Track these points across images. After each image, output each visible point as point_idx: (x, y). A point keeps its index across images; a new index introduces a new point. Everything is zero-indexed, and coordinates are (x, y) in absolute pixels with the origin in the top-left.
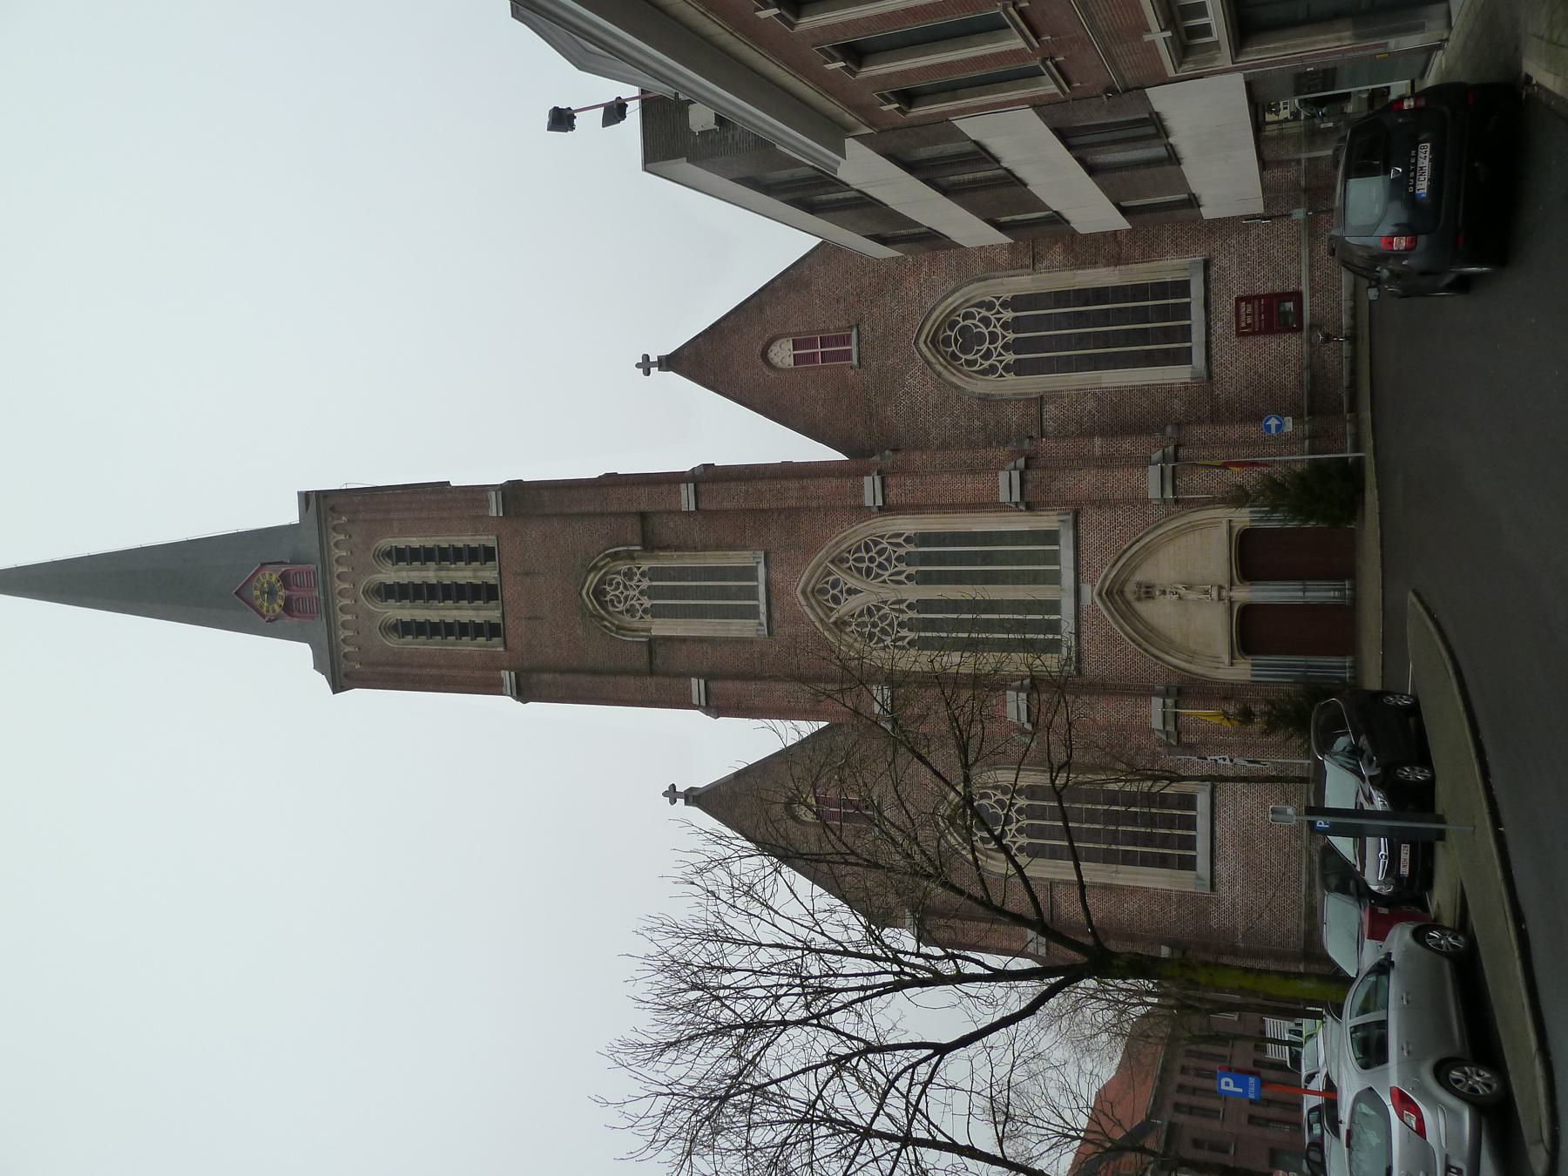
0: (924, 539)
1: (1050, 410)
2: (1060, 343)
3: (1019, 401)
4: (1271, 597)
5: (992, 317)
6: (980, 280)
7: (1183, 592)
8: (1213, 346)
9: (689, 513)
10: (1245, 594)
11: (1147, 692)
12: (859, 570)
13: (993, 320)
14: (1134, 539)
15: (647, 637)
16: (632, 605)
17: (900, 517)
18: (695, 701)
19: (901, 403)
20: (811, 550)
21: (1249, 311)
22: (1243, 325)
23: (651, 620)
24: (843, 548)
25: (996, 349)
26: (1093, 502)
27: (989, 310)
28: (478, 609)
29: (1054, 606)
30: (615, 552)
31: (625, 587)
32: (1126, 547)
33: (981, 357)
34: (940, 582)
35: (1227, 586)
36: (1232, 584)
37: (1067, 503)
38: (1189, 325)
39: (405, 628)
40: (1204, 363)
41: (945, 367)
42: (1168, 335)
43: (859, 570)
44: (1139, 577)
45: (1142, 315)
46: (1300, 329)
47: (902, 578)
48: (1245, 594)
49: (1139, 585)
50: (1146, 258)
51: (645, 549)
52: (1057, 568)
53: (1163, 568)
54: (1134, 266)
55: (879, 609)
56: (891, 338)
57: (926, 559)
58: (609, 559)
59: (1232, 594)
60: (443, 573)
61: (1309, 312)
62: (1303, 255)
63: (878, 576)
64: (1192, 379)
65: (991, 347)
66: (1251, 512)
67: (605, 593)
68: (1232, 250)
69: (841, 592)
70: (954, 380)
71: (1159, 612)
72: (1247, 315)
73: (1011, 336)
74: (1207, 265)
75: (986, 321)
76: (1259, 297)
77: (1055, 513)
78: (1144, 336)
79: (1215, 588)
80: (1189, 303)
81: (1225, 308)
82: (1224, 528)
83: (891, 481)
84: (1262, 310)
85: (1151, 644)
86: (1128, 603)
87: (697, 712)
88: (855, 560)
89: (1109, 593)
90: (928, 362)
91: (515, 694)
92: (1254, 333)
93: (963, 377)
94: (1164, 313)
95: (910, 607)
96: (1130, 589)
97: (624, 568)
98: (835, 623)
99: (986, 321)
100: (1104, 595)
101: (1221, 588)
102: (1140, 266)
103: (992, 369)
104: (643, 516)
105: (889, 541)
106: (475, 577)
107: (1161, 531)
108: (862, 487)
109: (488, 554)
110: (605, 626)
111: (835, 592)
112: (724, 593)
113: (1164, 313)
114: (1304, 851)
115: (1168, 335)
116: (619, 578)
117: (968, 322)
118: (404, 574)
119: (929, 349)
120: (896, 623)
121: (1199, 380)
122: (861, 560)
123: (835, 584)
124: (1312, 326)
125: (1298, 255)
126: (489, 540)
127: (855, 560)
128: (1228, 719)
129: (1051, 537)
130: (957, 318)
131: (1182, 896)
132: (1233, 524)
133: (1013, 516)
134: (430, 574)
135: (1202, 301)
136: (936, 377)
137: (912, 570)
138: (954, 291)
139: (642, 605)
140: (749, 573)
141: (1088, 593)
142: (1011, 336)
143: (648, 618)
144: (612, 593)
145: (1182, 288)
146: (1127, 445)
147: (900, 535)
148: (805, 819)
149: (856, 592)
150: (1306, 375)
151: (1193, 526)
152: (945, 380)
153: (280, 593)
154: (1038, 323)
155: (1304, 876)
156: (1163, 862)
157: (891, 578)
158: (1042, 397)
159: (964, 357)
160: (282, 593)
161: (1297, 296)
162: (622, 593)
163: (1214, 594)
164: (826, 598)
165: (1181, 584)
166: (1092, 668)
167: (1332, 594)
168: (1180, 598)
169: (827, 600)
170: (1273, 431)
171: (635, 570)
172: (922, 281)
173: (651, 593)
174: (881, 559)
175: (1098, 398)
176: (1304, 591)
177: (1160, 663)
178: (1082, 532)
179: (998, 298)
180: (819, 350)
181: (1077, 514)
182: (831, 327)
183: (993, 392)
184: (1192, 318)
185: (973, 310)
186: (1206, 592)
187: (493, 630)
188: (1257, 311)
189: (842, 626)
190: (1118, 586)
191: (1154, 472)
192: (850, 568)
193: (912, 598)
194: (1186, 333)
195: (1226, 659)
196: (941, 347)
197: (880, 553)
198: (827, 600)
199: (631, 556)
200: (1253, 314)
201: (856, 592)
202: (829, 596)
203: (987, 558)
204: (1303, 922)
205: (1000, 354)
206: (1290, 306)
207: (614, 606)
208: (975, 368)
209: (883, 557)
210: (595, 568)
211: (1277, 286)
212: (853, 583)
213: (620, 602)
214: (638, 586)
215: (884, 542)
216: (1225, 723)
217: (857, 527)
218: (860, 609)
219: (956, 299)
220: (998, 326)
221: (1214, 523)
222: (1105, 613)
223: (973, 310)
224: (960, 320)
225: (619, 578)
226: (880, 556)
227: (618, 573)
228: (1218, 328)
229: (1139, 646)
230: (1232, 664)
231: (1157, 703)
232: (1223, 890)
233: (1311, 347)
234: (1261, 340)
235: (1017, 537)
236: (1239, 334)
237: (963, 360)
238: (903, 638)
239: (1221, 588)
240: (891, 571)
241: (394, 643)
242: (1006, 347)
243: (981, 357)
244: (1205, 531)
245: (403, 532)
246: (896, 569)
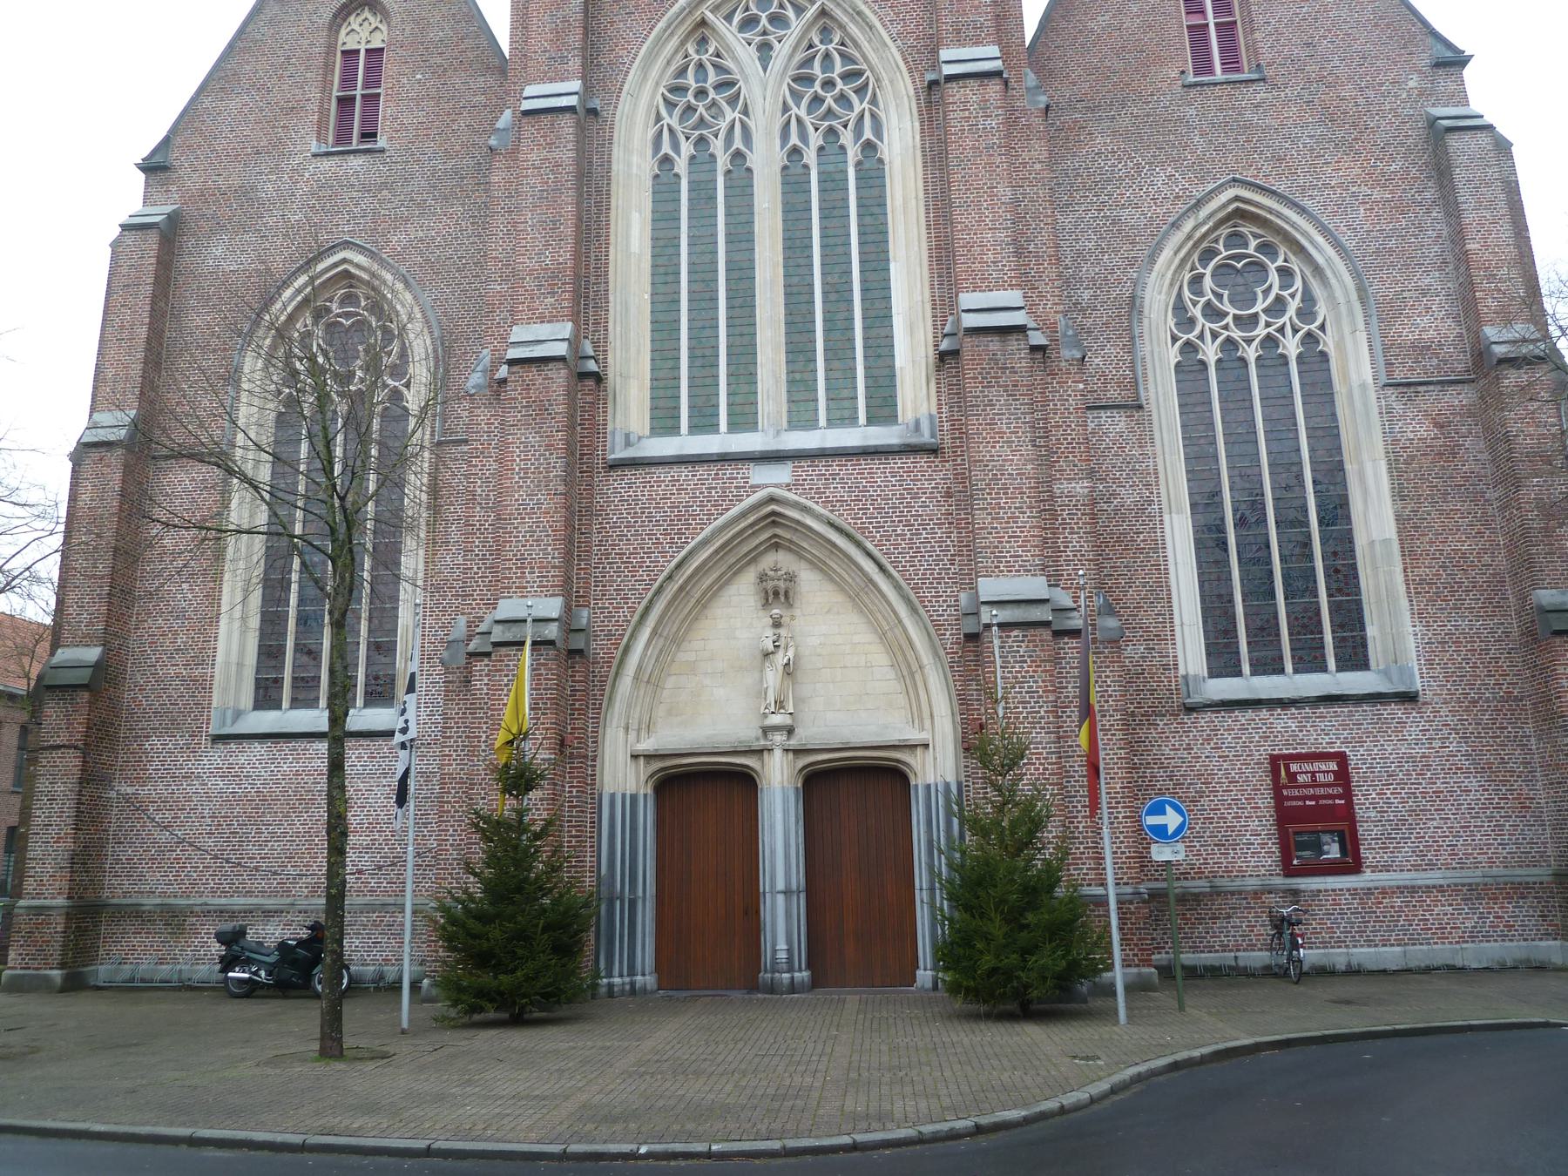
1: (1117, 424)
2: (1242, 439)
3: (1133, 368)
4: (772, 827)
5: (1285, 319)
6: (1361, 290)
7: (780, 659)
8: (1250, 714)
11: (573, 592)
12: (808, 62)
13: (1281, 321)
14: (884, 561)
17: (917, 124)
19: (1120, 159)
21: (1321, 778)
22: (1294, 767)
24: (853, 29)
25: (1226, 327)
26: (962, 478)
27: (1299, 313)
29: (744, 418)
32: (869, 546)
34: (788, 209)
35: (794, 743)
36: (797, 752)
37: (960, 431)
38: (1282, 671)
40: (1217, 697)
41: (1189, 237)
42: (1263, 632)
43: (808, 62)
44: (809, 581)
45: (1300, 584)
46: (1289, 871)
49: (791, 578)
50: (1416, 587)
52: (822, 421)
54: (1399, 568)
55: (733, 101)
56: (1242, 139)
57: (833, 183)
59: (778, 753)
61: (1322, 887)
62: (1430, 874)
63: (798, 97)
64: (1185, 677)
65: (1229, 319)
66: (947, 785)
68: (1436, 744)
69: (765, 33)
70: (1167, 253)
72: (1313, 773)
73: (1251, 353)
74: (1408, 698)
75: (1278, 307)
76: (1348, 795)
77: (934, 411)
78: (1260, 590)
79: (788, 720)
80: (1324, 669)
81: (1324, 733)
82: (914, 735)
83: (994, 87)
84: (1321, 802)
85: (670, 603)
86: (753, 558)
88: (827, 56)
89: (774, 519)
90: (1199, 204)
92: (1277, 788)
93: (1173, 267)
94: (1306, 624)
96: (783, 560)
98: (703, 23)
99: (1278, 307)
100: (774, 507)
101: (790, 731)
102: (1399, 578)
103: (1187, 323)
107: (903, 611)
111: (764, 21)
113: (1306, 624)
114: (289, 901)
115: (1263, 632)
117: (1274, 278)
119: (1224, 206)
121: (1183, 689)
124: (1295, 893)
125: (1432, 866)
128: (510, 743)
129: (883, 408)
130: (1281, 258)
131: (202, 685)
132: (919, 751)
133: (925, 334)
135: (1335, 691)
136: (1171, 220)
138: (1337, 245)
141: (774, 478)
142: (1251, 353)
145: (1354, 656)
146: (1076, 542)
147: (878, 130)
148: (343, 32)
149: (765, 62)
150: (1200, 885)
151: (912, 674)
152: (1166, 235)
154: (1278, 401)
155: (242, 901)
156: (270, 652)
158: (1140, 407)
159: (1208, 271)
161: (1351, 864)
163: (776, 720)
164: (752, 5)
166: (618, 487)
167: (782, 945)
168: (767, 655)
169: (747, 9)
170: (1152, 820)
172: (1354, 189)
174: (829, 101)
175: (1142, 507)
176: (787, 892)
177: (636, 617)
178: (898, 463)
179: (1322, 327)
181: (933, 451)
183: (1146, 321)
184: (1298, 676)
185: (1298, 284)
186: (780, 704)
188: (1322, 791)
189: (697, 35)
190: (788, 536)
191: (1035, 586)
193: (755, 160)
194: (1268, 665)
195: (646, 745)
196: (1224, 231)
197: (842, 99)
200: (1315, 784)
201: (765, 62)
203: (837, 293)
204: (158, 901)
205: (1215, 335)
206: (1333, 851)
208: (1187, 293)
209: (834, 106)
211: (1368, 831)
212: (781, 51)
215: (865, 105)
216: (501, 737)
217: (894, 50)
219: (1323, 252)
220: (1270, 329)
221: (918, 714)
222: (734, 511)
223: (1298, 284)
224: (1280, 262)
228: (1284, 722)
229: (670, 577)
230: (635, 757)
231: (552, 606)
232: (216, 757)
233: (1256, 893)
234: (1265, 801)
235: (880, 348)
236: (1274, 760)
237: (1202, 271)
238: (676, 146)
239: (790, 731)
240: (807, 120)
242: (1230, 343)
243: (1208, 304)
244: (902, 700)
246: (811, 129)
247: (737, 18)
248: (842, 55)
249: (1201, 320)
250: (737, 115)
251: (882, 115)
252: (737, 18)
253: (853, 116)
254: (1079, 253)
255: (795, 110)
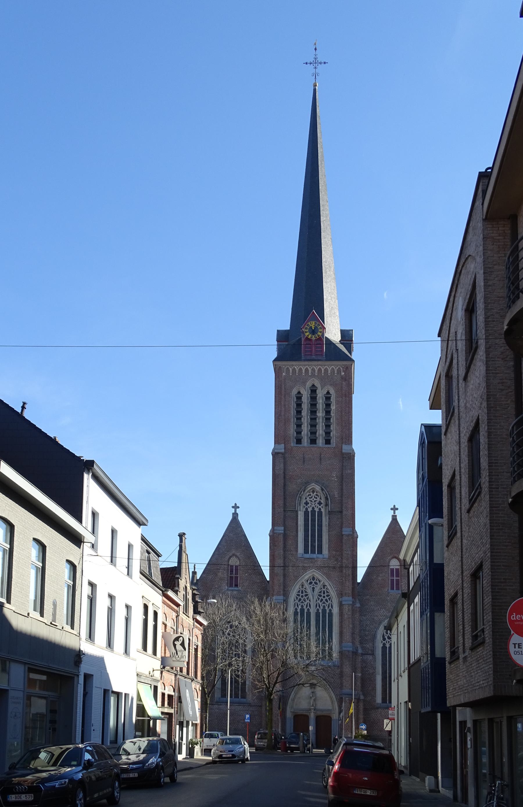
0: (331, 615)
1: (370, 657)
3: (373, 648)
7: (313, 698)
9: (341, 531)
10: (312, 716)
15: (298, 509)
16: (309, 503)
18: (275, 528)
20: (329, 577)
23: (304, 511)
28: (307, 435)
30: (328, 499)
31: (315, 501)
33: (389, 636)
39: (299, 397)
43: (321, 592)
47: (318, 607)
48: (312, 716)
51: (329, 512)
53: (320, 692)
58: (326, 496)
59: (312, 713)
60: (321, 420)
63: (319, 599)
67: (313, 492)
69: (313, 585)
71: (306, 691)
87: (270, 527)
88: (324, 591)
91: (276, 451)
95: (308, 610)
97: (322, 501)
103: (384, 639)
104: (341, 512)
105: (330, 604)
106: (319, 435)
108: (349, 596)
109: (328, 442)
110: (301, 492)
112: (313, 541)
116: (318, 499)
118: (321, 401)
120: (303, 604)
122: (324, 593)
123: (316, 583)
126: (333, 441)
127: (324, 591)
134: (320, 414)
137: (320, 611)
139: (309, 507)
140: (320, 552)
143: (304, 510)
144: (313, 495)
147: (332, 607)
153: (313, 336)
157: (318, 603)
160: (314, 338)
162: (313, 499)
165: (316, 697)
168: (311, 697)
169: (310, 580)
171: (322, 505)
173: (313, 511)
180: (395, 578)
182: (402, 584)
186: (313, 705)
187: (299, 441)
192: (321, 589)
197: (327, 601)
198: (310, 580)
199: (327, 505)
202: (312, 581)
205: (389, 642)
207: (308, 496)
208: (385, 633)
210: (322, 490)
212: (317, 590)
213: (310, 498)
214: (315, 506)
218: (308, 592)
225: (318, 499)
226: (325, 600)
227: (321, 499)
230: (291, 712)
241: (294, 392)
243: (388, 636)
245: (337, 402)
247: (309, 582)
248: (326, 591)
249: (387, 639)
250: (308, 601)
251: (333, 604)
252: (309, 582)
253: (328, 604)
254: (366, 625)
255: (318, 601)
